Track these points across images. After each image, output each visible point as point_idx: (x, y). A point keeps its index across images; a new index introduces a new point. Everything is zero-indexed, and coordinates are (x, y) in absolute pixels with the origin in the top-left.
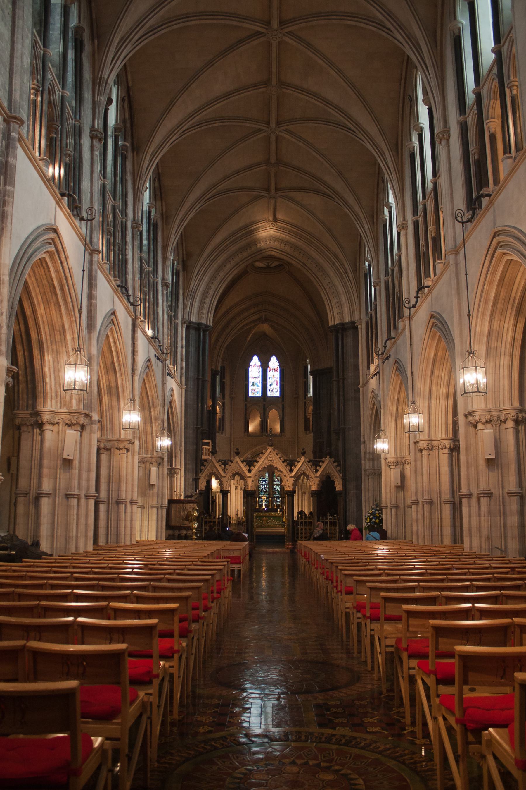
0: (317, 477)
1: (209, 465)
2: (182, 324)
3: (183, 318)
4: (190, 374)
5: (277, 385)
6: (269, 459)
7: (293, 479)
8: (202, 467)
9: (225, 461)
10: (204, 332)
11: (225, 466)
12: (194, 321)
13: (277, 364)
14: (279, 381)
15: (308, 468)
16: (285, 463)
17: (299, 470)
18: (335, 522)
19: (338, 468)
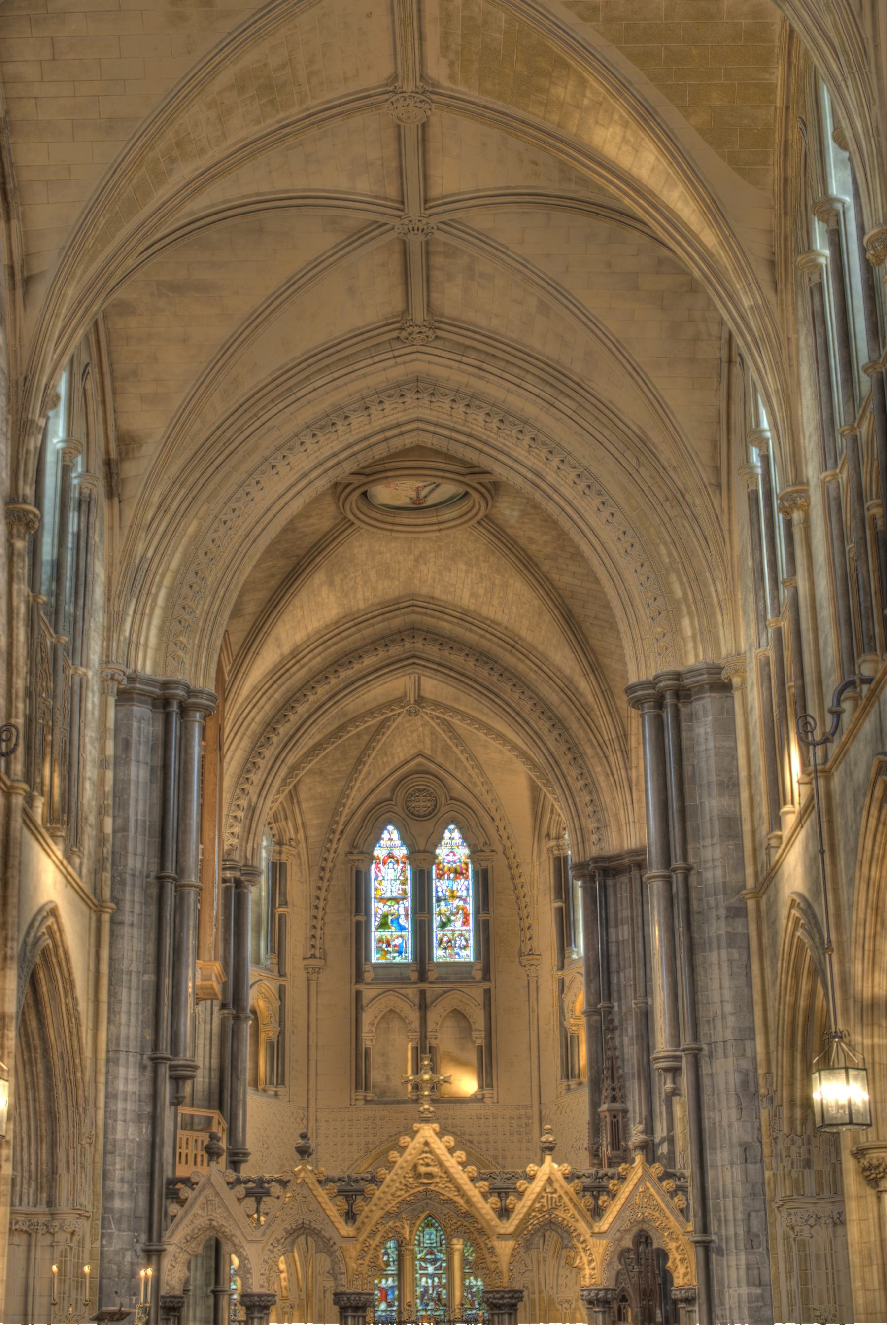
0: (600, 1234)
1: (201, 1199)
2: (103, 681)
3: (106, 660)
4: (130, 862)
5: (465, 923)
9: (261, 1182)
10: (184, 710)
11: (258, 1201)
12: (148, 670)
13: (463, 852)
14: (470, 909)
19: (679, 1201)
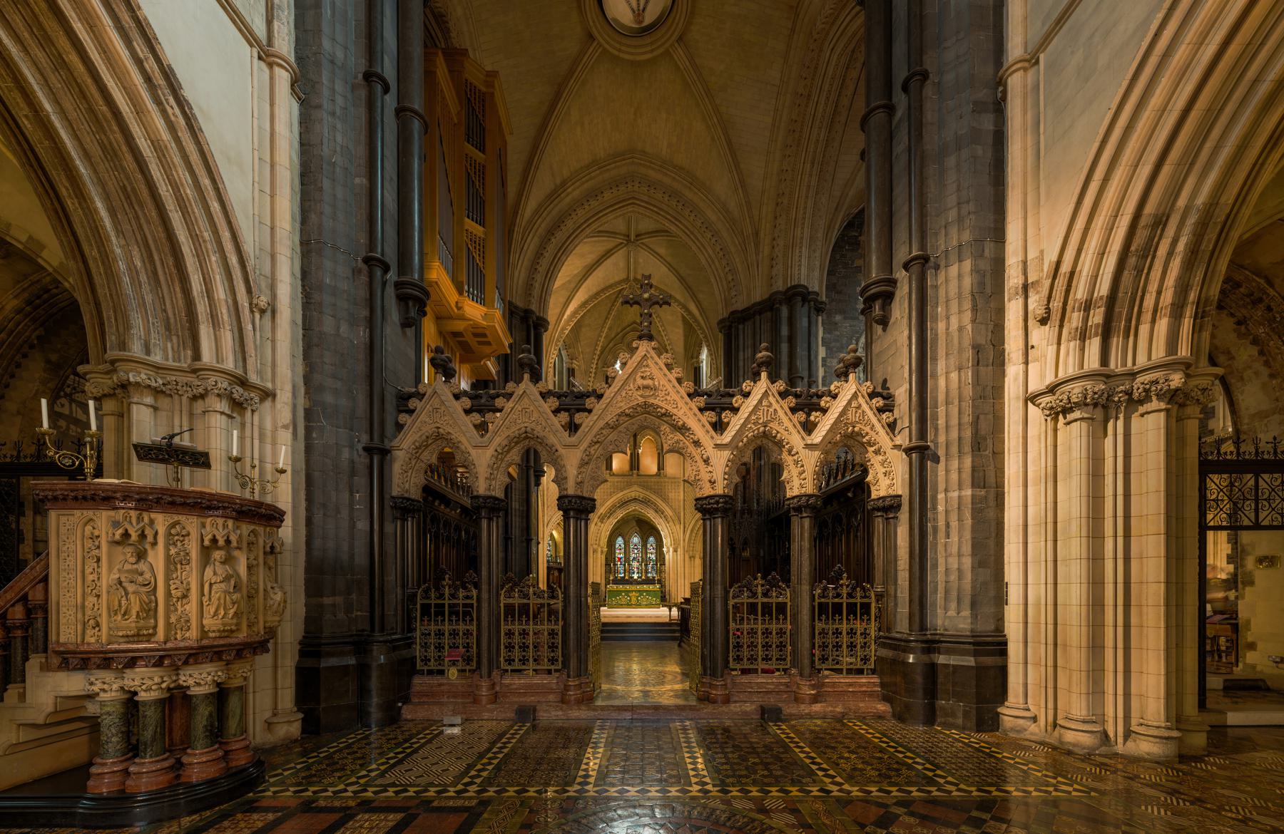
0: (810, 447)
6: (640, 382)
7: (726, 454)
8: (403, 418)
15: (781, 413)
16: (701, 401)
17: (747, 420)
18: (866, 608)
